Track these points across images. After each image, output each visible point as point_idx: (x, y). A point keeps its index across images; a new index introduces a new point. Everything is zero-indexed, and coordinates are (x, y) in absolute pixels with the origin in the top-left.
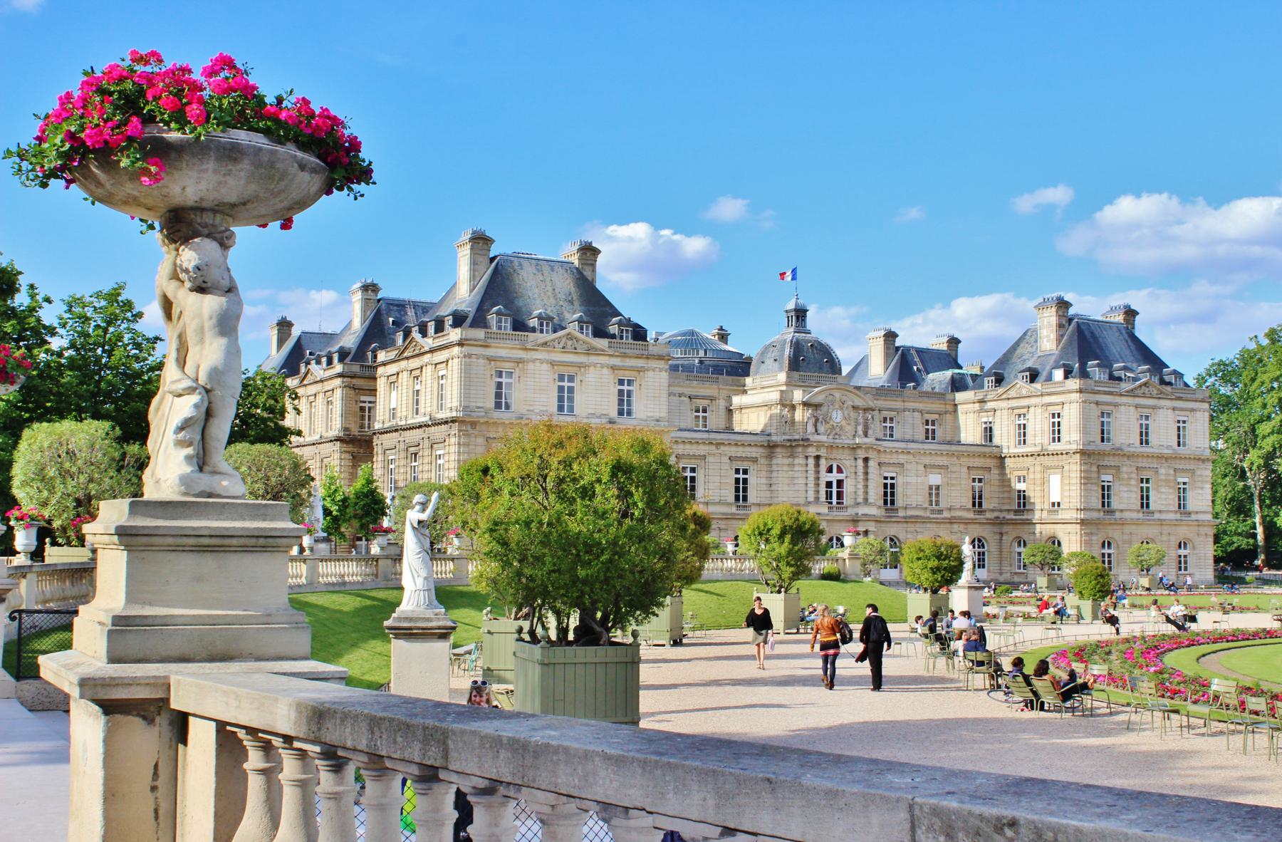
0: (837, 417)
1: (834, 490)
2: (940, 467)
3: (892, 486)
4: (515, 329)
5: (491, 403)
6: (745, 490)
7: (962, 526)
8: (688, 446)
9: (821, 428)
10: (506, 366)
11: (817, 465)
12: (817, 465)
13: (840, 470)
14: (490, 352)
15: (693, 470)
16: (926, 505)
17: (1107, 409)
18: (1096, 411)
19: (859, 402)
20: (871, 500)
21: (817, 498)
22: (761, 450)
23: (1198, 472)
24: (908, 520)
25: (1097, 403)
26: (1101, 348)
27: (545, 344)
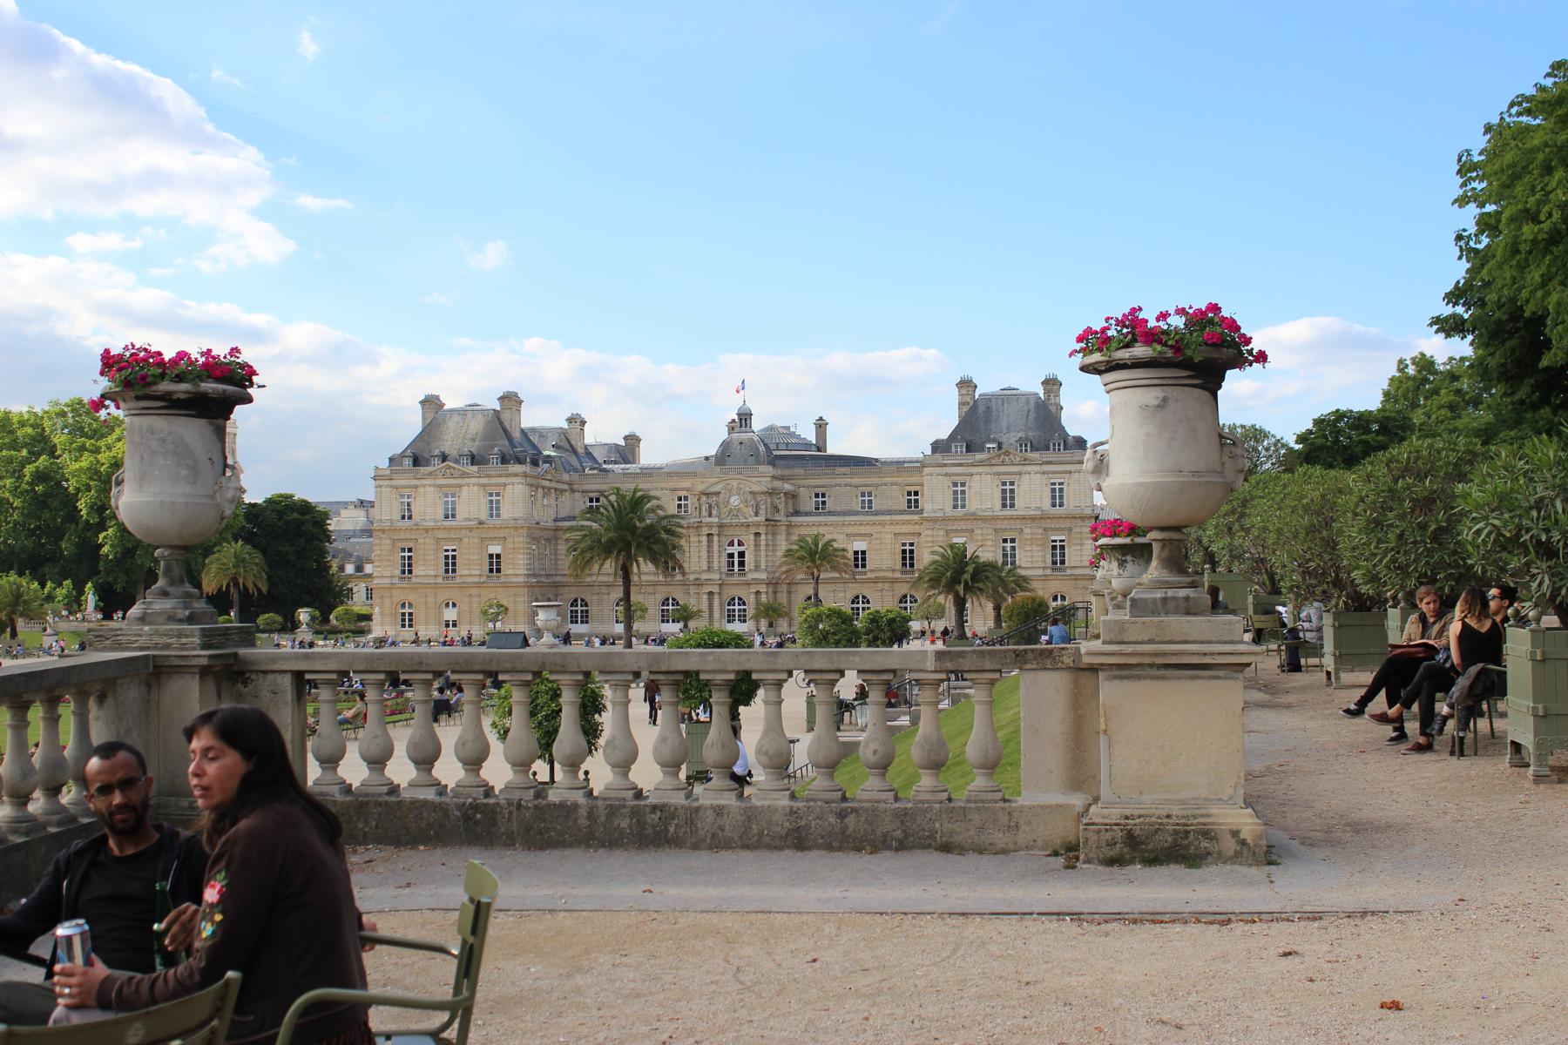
0: (735, 501)
1: (736, 560)
4: (417, 462)
5: (397, 516)
7: (887, 586)
10: (406, 491)
11: (710, 541)
12: (710, 541)
14: (394, 483)
17: (959, 479)
18: (948, 482)
19: (756, 488)
21: (710, 569)
23: (1076, 530)
26: (988, 420)
27: (430, 474)
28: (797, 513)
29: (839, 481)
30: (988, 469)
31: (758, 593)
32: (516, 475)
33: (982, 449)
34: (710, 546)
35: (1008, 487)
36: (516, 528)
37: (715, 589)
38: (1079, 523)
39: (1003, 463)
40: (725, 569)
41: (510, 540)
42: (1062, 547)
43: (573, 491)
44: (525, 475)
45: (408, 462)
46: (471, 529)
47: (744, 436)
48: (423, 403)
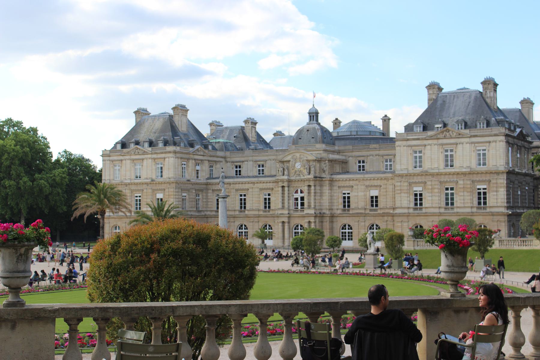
0: (298, 166)
1: (299, 202)
2: (376, 186)
3: (349, 198)
6: (269, 203)
7: (390, 218)
8: (240, 185)
9: (286, 173)
11: (283, 190)
12: (283, 190)
13: (301, 192)
14: (111, 158)
15: (245, 195)
16: (369, 206)
17: (418, 149)
19: (311, 158)
20: (312, 206)
21: (283, 207)
22: (274, 184)
23: (493, 181)
24: (354, 215)
25: (408, 146)
27: (128, 152)
28: (347, 172)
29: (371, 153)
30: (435, 142)
31: (309, 222)
32: (170, 152)
33: (432, 129)
34: (283, 194)
35: (449, 153)
36: (169, 183)
37: (286, 220)
38: (496, 176)
39: (445, 137)
40: (292, 207)
41: (167, 190)
42: (485, 193)
43: (227, 162)
44: (175, 152)
45: (119, 147)
46: (147, 184)
47: (311, 126)
48: (136, 112)
